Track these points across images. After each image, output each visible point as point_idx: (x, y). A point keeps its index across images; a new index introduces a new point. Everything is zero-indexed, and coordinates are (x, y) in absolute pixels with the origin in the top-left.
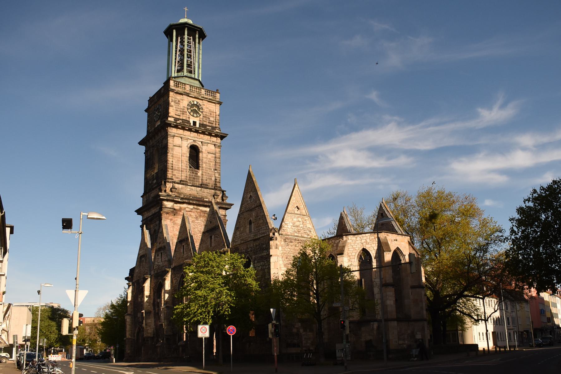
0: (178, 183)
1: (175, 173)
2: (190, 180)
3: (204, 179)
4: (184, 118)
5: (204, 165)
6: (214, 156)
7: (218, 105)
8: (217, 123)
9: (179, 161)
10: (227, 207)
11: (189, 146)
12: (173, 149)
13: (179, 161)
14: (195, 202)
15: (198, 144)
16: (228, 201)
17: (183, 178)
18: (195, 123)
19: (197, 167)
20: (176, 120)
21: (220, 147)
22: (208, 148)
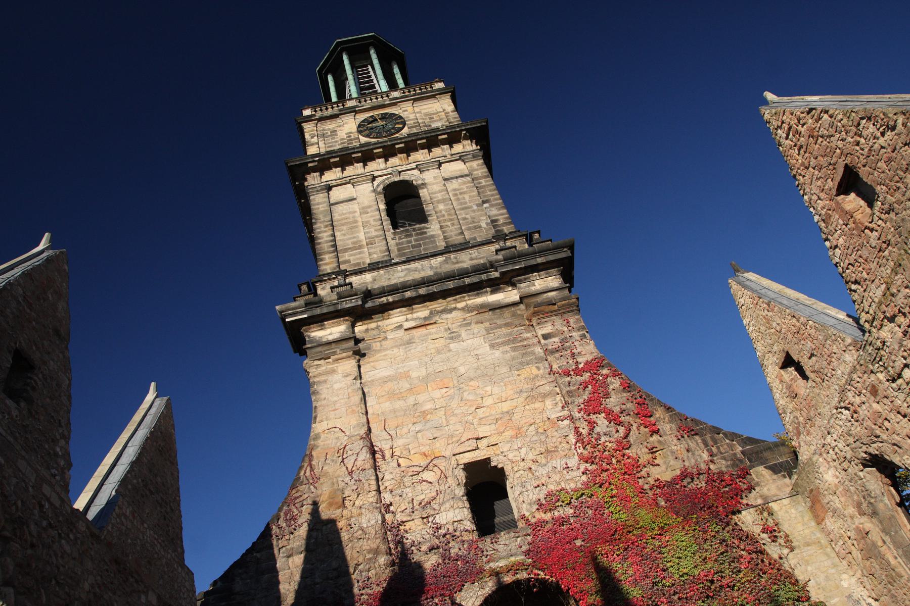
2: (400, 256)
5: (441, 207)
6: (468, 179)
9: (357, 227)
15: (413, 176)
19: (422, 218)
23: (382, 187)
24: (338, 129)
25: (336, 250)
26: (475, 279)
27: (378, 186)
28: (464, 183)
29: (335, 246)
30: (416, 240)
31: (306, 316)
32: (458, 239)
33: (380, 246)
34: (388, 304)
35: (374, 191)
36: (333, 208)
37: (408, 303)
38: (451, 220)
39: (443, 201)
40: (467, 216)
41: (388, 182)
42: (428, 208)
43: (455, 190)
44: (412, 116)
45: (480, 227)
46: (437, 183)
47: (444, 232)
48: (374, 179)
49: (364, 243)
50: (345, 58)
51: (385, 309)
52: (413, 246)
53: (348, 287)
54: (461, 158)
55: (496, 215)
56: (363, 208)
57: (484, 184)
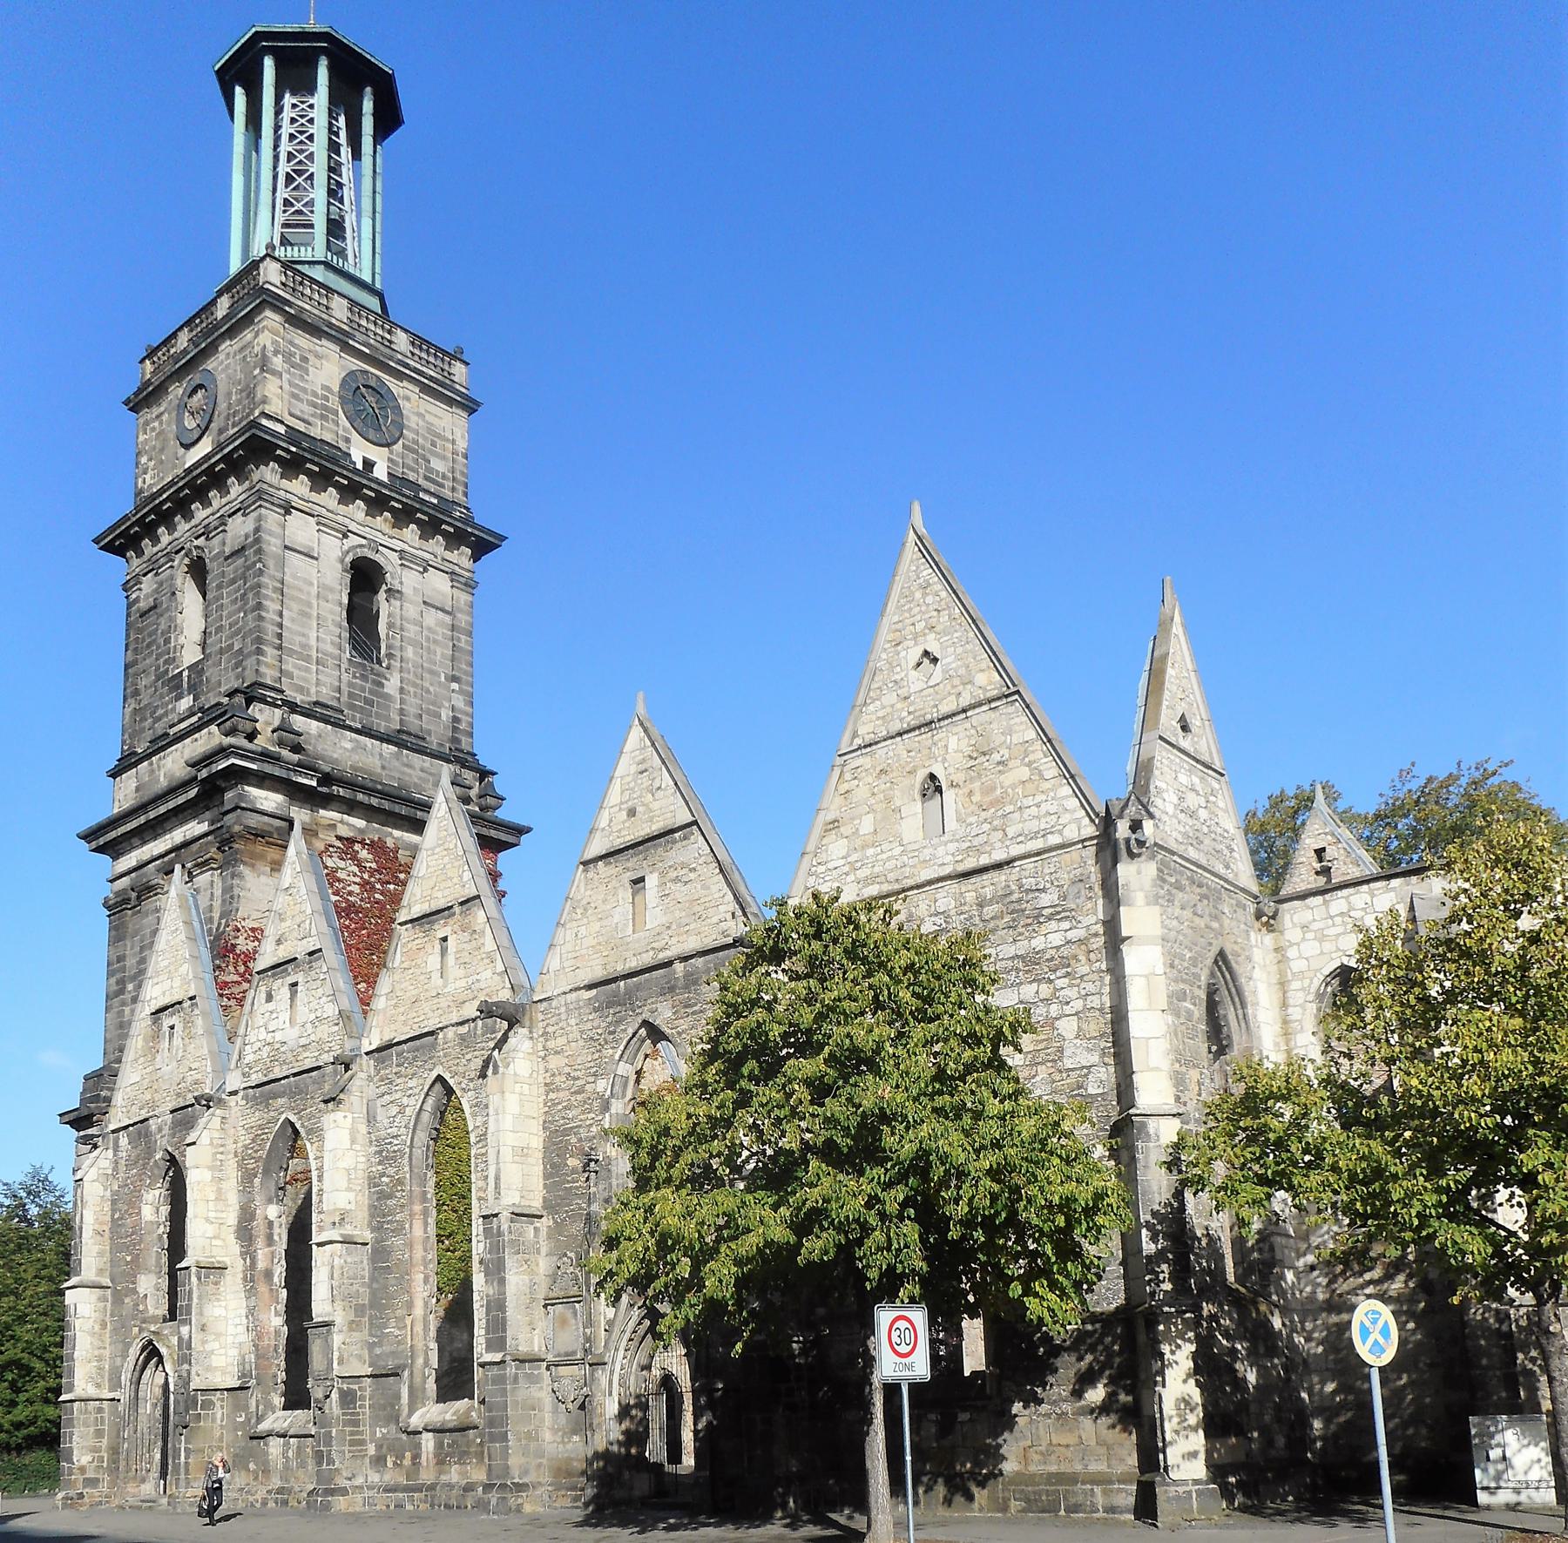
1: (290, 664)
2: (352, 707)
3: (412, 710)
4: (328, 437)
5: (410, 652)
6: (448, 619)
7: (465, 414)
10: (503, 837)
11: (349, 559)
12: (282, 564)
13: (307, 615)
14: (374, 802)
15: (389, 561)
16: (502, 814)
17: (326, 694)
18: (369, 465)
20: (294, 435)
21: (470, 586)
22: (421, 583)
24: (311, 357)
29: (280, 636)
32: (413, 724)
33: (329, 677)
37: (351, 807)
38: (415, 685)
41: (360, 553)
43: (429, 629)
47: (402, 701)
48: (345, 536)
51: (325, 801)
52: (367, 701)
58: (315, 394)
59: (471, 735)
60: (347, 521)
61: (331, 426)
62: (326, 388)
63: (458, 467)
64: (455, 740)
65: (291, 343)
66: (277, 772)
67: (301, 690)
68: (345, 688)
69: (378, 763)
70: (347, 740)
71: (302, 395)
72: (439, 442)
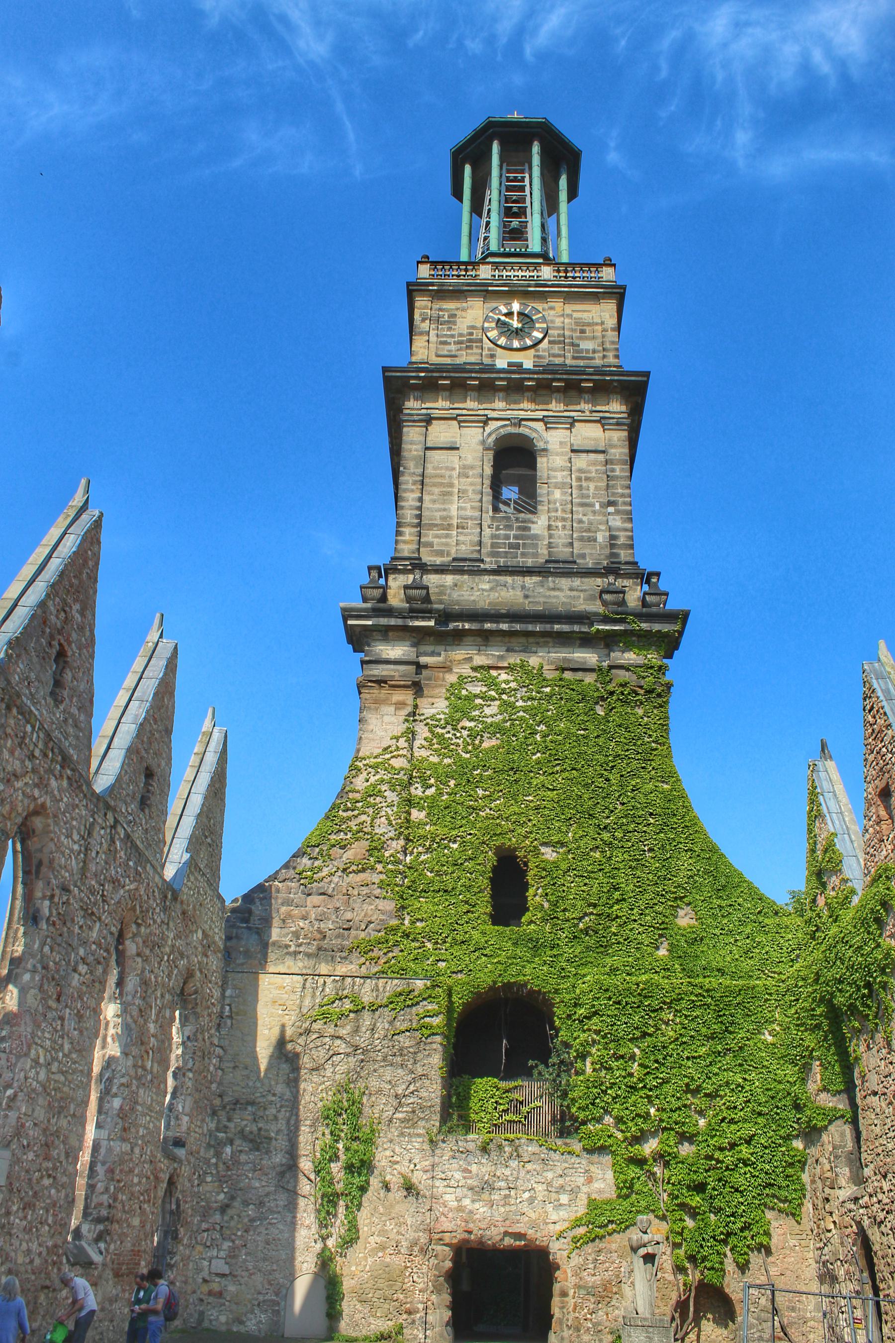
0: (441, 570)
2: (494, 554)
4: (472, 359)
5: (557, 494)
6: (601, 457)
8: (611, 354)
9: (450, 494)
11: (491, 440)
14: (504, 626)
17: (466, 549)
23: (493, 437)
24: (459, 313)
25: (419, 525)
26: (566, 628)
27: (490, 435)
28: (594, 463)
29: (419, 517)
30: (516, 537)
31: (370, 623)
32: (562, 552)
34: (464, 630)
35: (483, 442)
36: (428, 453)
39: (561, 486)
40: (585, 519)
41: (502, 431)
42: (542, 490)
43: (580, 471)
44: (558, 322)
45: (595, 540)
46: (562, 454)
48: (485, 423)
49: (455, 522)
50: (496, 147)
52: (511, 546)
53: (424, 592)
54: (602, 422)
55: (619, 529)
56: (465, 467)
57: (617, 473)
58: (461, 335)
59: (631, 547)
60: (486, 412)
61: (475, 350)
62: (473, 327)
63: (607, 339)
64: (613, 555)
65: (440, 310)
66: (393, 622)
67: (440, 553)
68: (487, 540)
69: (519, 593)
70: (485, 583)
71: (449, 340)
72: (587, 329)
